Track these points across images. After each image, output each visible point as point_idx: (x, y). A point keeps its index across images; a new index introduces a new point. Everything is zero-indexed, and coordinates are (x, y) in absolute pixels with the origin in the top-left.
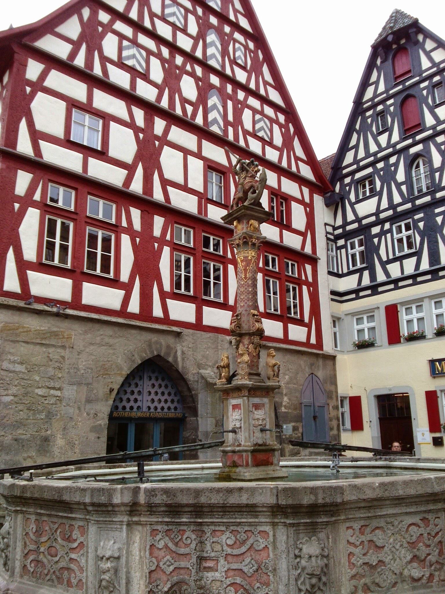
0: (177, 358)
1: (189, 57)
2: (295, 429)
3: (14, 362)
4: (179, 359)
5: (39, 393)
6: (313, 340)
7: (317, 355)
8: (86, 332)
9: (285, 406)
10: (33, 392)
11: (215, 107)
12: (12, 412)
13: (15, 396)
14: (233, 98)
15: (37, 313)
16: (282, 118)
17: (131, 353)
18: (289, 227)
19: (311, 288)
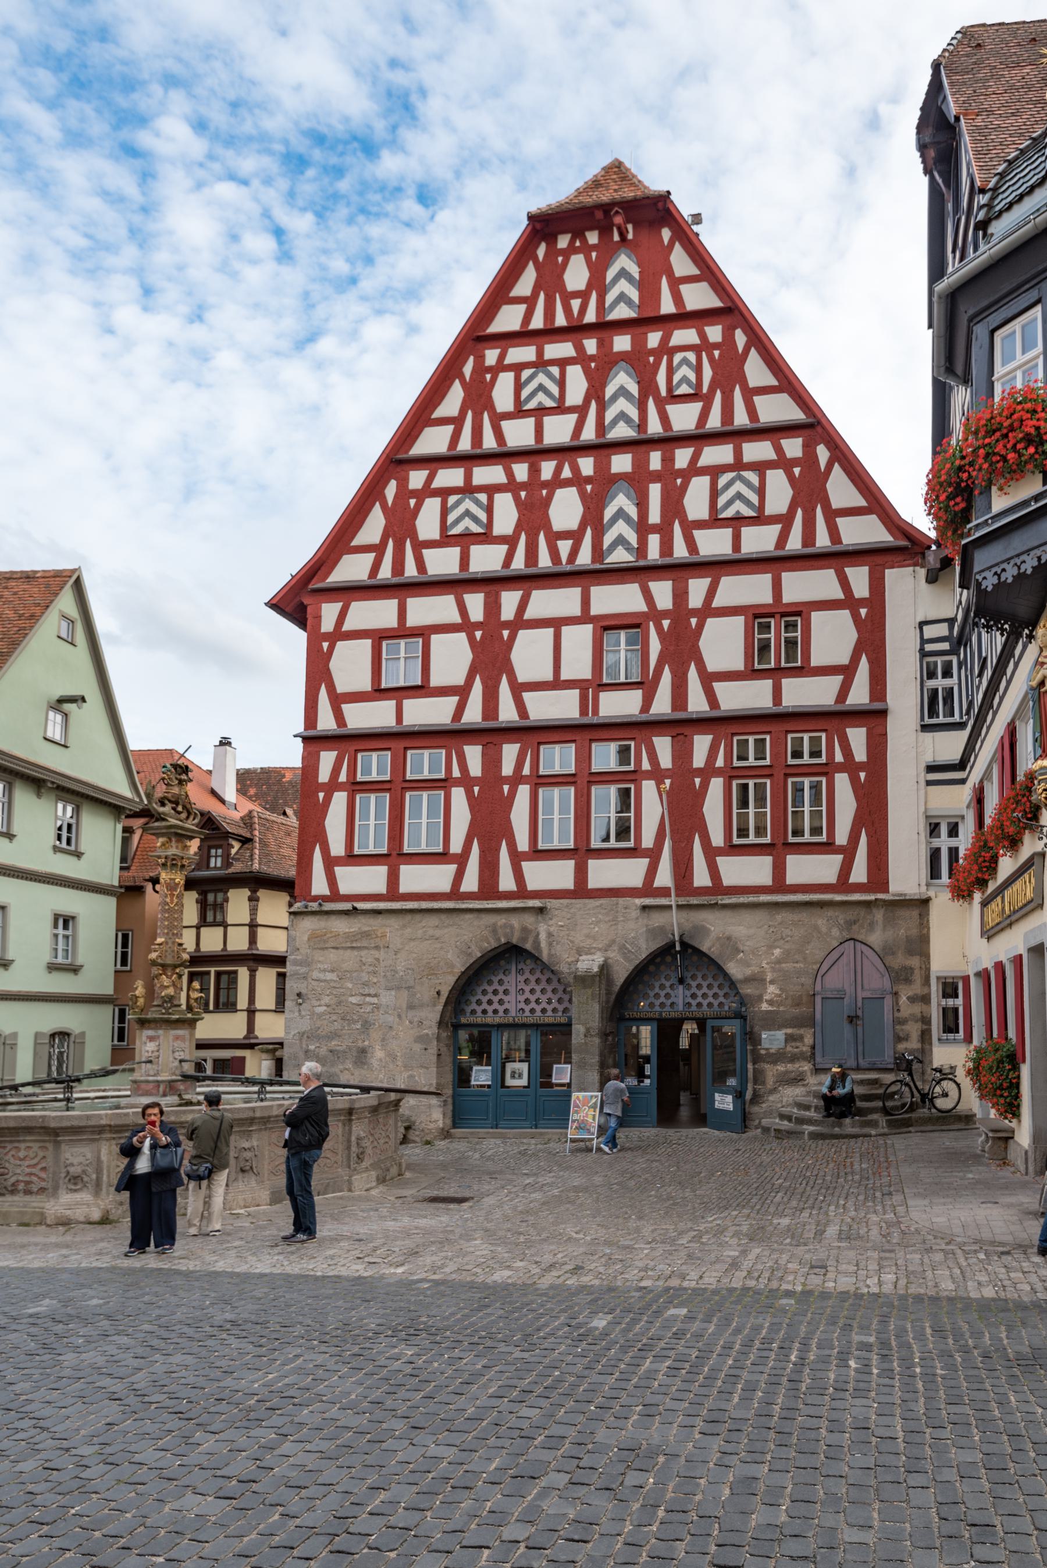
0: (539, 944)
2: (789, 1038)
3: (325, 971)
4: (543, 945)
7: (867, 904)
8: (404, 926)
9: (770, 1002)
10: (347, 1001)
11: (620, 514)
12: (325, 1022)
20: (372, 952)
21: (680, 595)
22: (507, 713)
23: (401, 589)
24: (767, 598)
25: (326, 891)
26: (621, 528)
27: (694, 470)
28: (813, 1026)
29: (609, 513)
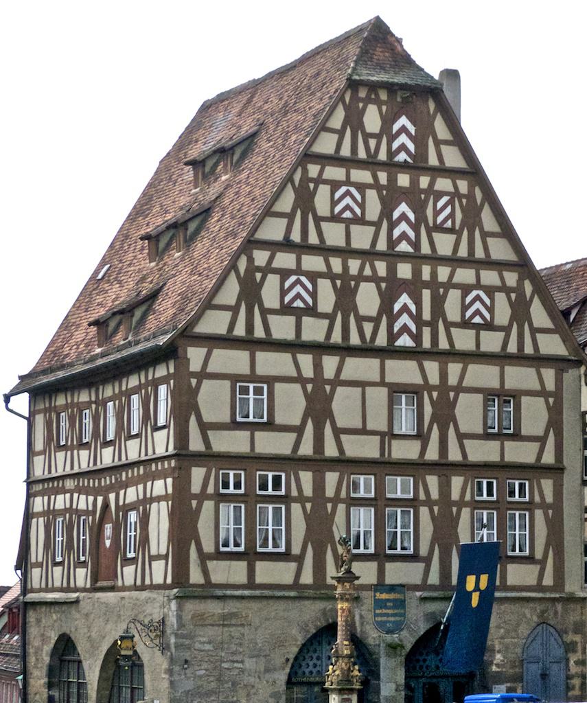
0: (355, 622)
1: (369, 255)
2: (509, 690)
4: (358, 624)
5: (226, 667)
6: (548, 581)
7: (554, 600)
8: (260, 610)
9: (498, 665)
11: (405, 308)
13: (206, 670)
14: (433, 284)
15: (218, 599)
16: (511, 278)
17: (305, 624)
18: (516, 436)
19: (550, 512)
20: (240, 628)
21: (444, 375)
22: (331, 450)
23: (250, 343)
24: (495, 384)
25: (202, 581)
26: (405, 319)
27: (450, 285)
28: (522, 681)
29: (397, 307)
